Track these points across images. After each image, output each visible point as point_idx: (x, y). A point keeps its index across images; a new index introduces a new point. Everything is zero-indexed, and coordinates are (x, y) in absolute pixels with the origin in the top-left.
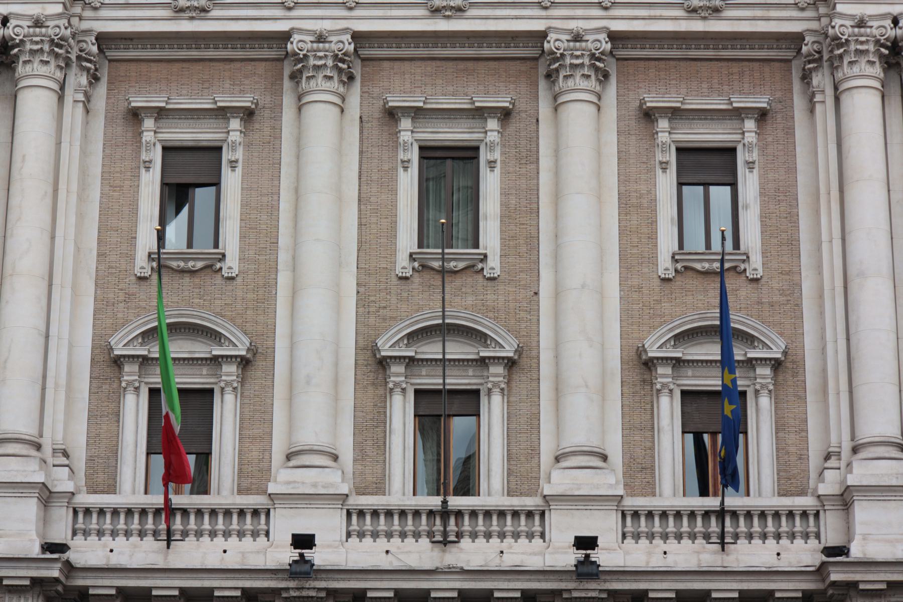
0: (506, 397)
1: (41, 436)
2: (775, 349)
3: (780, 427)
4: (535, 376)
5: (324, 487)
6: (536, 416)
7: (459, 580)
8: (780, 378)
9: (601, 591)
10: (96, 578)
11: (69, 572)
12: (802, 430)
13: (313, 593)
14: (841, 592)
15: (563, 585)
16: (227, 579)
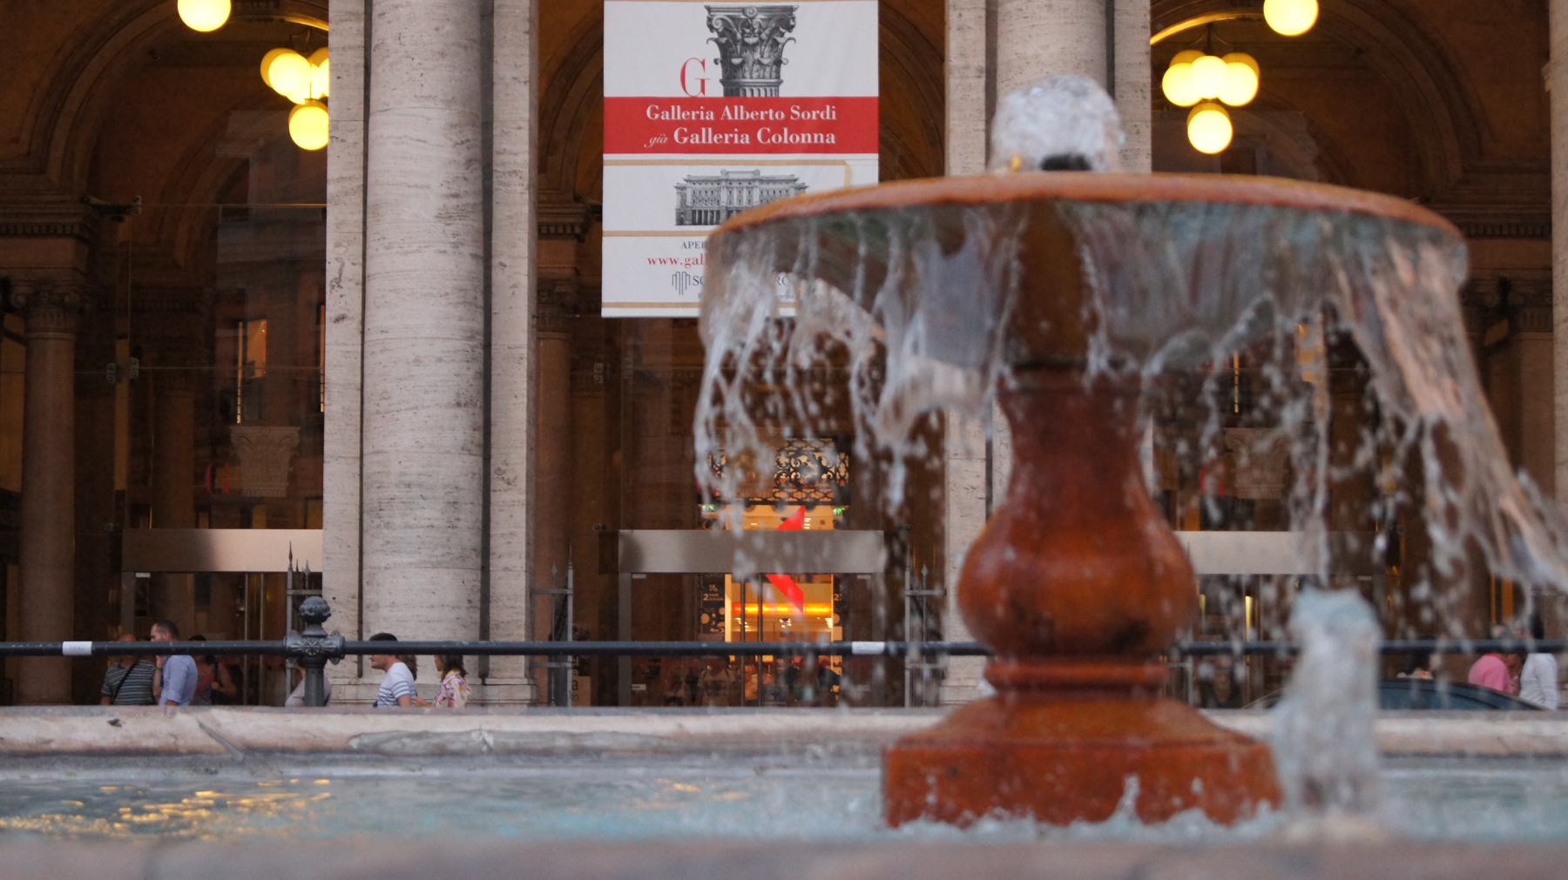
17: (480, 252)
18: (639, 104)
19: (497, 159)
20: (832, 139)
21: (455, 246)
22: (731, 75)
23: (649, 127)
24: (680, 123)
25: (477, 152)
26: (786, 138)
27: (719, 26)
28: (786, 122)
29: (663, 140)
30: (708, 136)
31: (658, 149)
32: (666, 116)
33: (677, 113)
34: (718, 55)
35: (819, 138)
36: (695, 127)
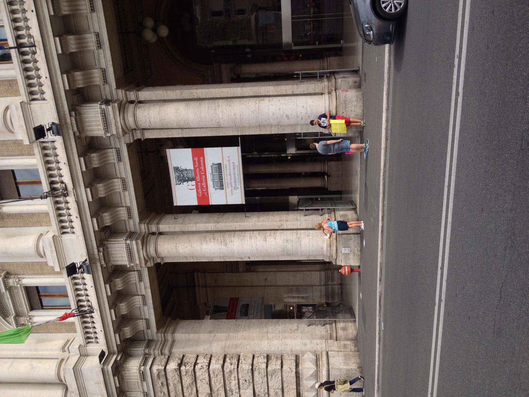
1: (58, 359)
7: (80, 189)
9: (71, 116)
10: (112, 343)
13: (101, 254)
15: (72, 137)
16: (101, 291)
17: (233, 233)
18: (198, 197)
19: (213, 230)
20: (202, 158)
21: (232, 242)
22: (189, 180)
23: (203, 195)
25: (211, 236)
26: (202, 168)
27: (180, 182)
28: (199, 168)
29: (206, 193)
30: (204, 184)
31: (208, 194)
32: (200, 193)
33: (200, 190)
34: (186, 182)
35: (202, 161)
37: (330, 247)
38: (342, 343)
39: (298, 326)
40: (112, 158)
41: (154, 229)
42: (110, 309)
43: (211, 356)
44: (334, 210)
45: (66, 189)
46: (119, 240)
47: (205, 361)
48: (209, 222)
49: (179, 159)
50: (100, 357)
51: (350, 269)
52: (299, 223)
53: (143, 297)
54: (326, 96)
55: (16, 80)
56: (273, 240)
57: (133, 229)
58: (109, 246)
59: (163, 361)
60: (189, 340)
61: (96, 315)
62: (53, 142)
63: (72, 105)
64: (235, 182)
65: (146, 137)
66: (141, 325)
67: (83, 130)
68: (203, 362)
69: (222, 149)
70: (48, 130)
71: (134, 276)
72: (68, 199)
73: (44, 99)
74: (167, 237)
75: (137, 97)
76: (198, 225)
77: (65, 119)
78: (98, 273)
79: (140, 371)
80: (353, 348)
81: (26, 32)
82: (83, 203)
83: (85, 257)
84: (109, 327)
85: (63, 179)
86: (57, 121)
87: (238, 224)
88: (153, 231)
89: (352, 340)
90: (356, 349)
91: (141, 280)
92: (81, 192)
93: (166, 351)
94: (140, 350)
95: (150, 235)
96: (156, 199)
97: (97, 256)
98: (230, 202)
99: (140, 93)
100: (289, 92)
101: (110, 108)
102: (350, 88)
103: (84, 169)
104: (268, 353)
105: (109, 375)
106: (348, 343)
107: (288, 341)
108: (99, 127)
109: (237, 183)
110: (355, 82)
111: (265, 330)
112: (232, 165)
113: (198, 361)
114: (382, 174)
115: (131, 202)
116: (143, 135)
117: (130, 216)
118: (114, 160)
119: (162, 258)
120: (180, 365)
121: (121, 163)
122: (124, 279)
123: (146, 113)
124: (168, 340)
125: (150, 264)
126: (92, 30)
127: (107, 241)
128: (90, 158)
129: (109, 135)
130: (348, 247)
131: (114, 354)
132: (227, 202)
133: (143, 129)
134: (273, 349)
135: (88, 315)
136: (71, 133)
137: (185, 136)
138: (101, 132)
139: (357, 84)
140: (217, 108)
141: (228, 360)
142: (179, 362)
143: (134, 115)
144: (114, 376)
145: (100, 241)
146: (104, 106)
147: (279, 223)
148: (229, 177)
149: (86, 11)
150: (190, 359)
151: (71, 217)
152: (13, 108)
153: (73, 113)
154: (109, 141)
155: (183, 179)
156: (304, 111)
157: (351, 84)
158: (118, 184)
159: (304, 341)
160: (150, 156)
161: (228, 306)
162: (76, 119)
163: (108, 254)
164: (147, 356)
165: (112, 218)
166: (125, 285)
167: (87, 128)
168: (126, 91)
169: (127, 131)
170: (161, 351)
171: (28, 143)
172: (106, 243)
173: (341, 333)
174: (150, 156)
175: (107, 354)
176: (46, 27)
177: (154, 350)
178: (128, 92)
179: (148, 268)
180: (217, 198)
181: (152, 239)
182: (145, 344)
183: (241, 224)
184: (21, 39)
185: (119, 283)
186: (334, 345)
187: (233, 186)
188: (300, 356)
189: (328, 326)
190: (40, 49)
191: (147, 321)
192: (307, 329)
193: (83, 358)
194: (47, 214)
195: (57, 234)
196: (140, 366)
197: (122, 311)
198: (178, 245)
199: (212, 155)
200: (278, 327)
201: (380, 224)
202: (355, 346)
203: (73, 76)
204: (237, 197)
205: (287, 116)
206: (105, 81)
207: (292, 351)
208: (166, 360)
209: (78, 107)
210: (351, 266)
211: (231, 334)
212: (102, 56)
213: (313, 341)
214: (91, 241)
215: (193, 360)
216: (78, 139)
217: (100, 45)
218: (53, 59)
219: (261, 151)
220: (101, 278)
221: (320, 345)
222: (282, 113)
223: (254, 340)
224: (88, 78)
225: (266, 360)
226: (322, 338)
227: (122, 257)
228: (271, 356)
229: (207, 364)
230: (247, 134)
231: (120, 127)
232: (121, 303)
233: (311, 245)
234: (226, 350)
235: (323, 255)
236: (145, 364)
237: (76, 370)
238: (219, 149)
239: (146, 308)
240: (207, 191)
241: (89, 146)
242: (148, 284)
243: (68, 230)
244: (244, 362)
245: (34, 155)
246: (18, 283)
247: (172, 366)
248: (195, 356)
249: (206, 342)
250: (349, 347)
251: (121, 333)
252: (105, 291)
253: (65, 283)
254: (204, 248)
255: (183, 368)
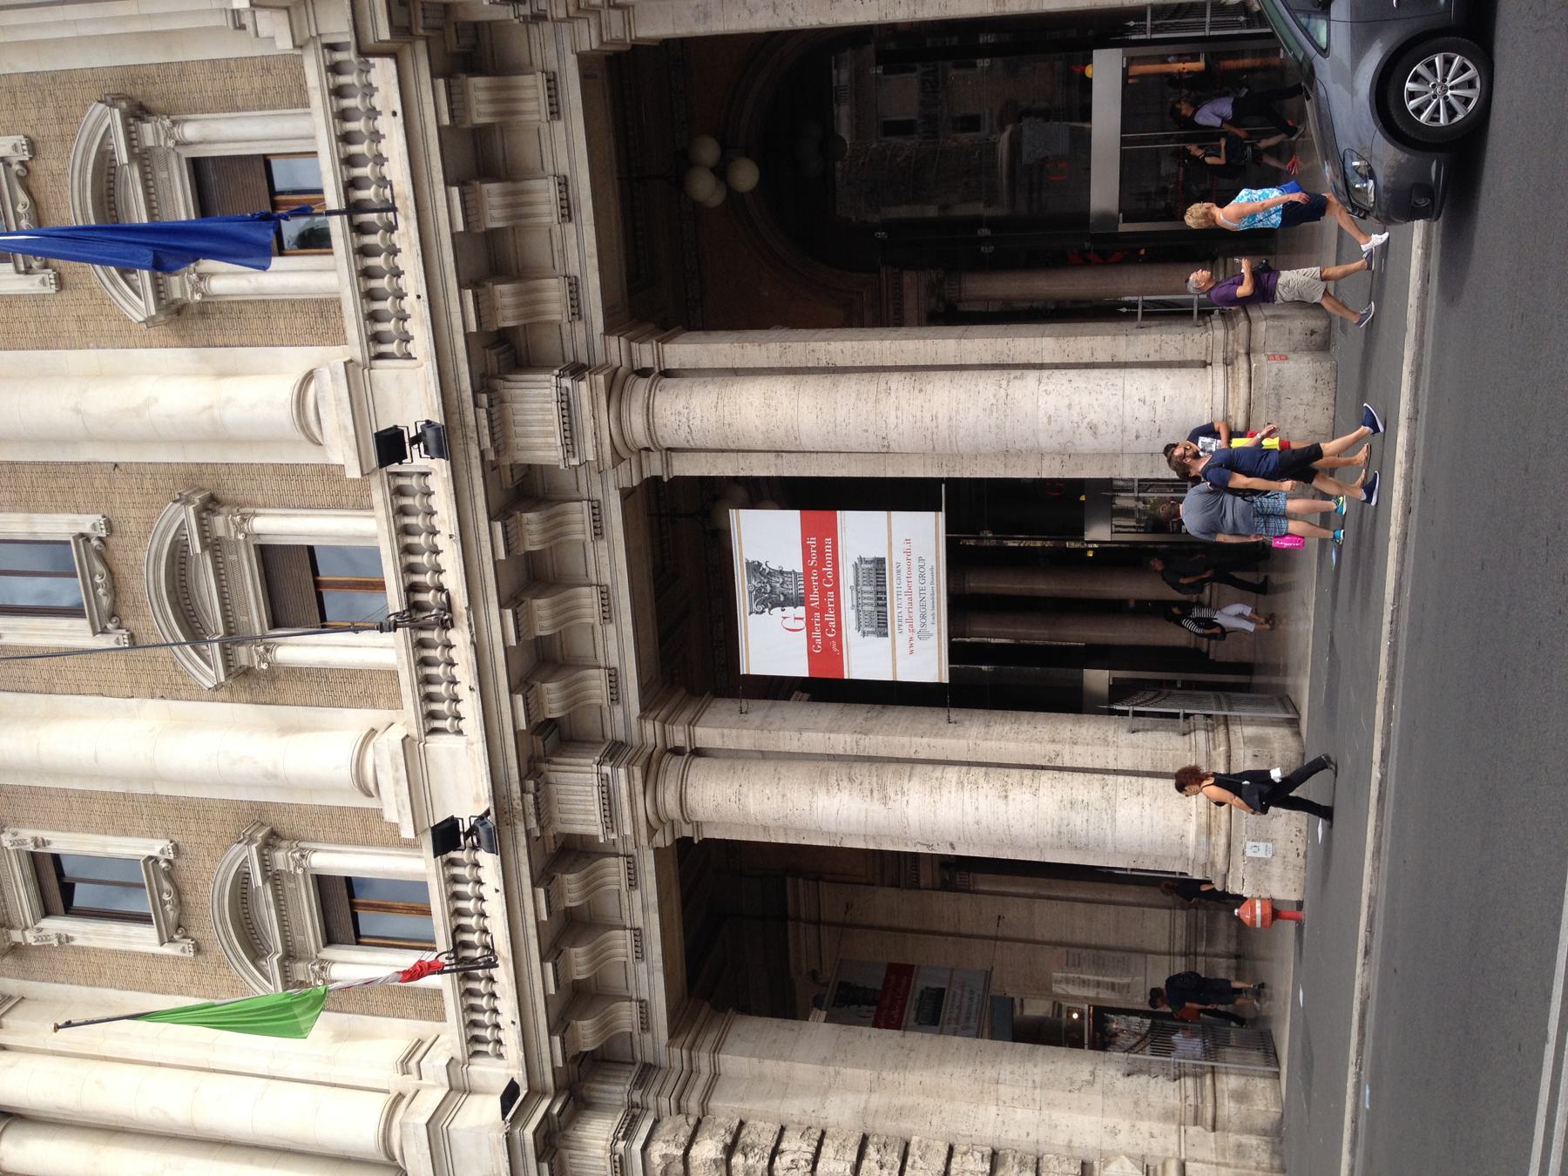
0: (259, 511)
1: (387, 1092)
2: (108, 120)
3: (229, 104)
4: (225, 469)
5: (397, 770)
6: (277, 468)
7: (487, 609)
8: (159, 104)
9: (476, 405)
10: (541, 1062)
11: (537, 1092)
12: (228, 66)
13: (531, 797)
14: (420, 14)
15: (476, 463)
16: (522, 906)
17: (908, 767)
23: (826, 648)
24: (823, 633)
26: (829, 569)
27: (761, 608)
30: (830, 617)
31: (840, 647)
33: (817, 634)
36: (825, 625)
37: (1209, 833)
38: (1233, 1138)
39: (1093, 1073)
40: (579, 527)
41: (679, 737)
42: (543, 960)
43: (823, 1133)
44: (1226, 721)
45: (449, 607)
46: (582, 761)
47: (804, 1147)
48: (838, 731)
49: (765, 538)
50: (502, 1098)
51: (1269, 911)
52: (1112, 752)
53: (638, 933)
54: (1218, 372)
55: (338, 300)
56: (1028, 796)
57: (621, 736)
58: (552, 777)
59: (681, 1133)
60: (761, 1078)
61: (503, 975)
62: (425, 474)
63: (483, 376)
64: (923, 617)
65: (676, 473)
66: (627, 1016)
67: (506, 445)
68: (797, 1147)
69: (889, 518)
70: (415, 440)
71: (615, 870)
72: (453, 635)
73: (408, 356)
74: (716, 763)
75: (659, 358)
76: (805, 735)
77: (462, 414)
78: (516, 851)
79: (613, 1153)
80: (1265, 1158)
81: (373, 170)
82: (492, 652)
83: (486, 804)
84: (535, 1012)
85: (442, 578)
86: (438, 419)
87: (925, 740)
88: (678, 744)
89: (1264, 1133)
90: (1276, 1163)
91: (633, 883)
92: (488, 615)
93: (693, 1104)
94: (617, 1091)
95: (668, 756)
96: (692, 650)
97: (517, 803)
98: (904, 676)
99: (667, 347)
100: (1102, 357)
101: (584, 386)
102: (1295, 351)
103: (502, 555)
104: (997, 1146)
105: (524, 1155)
106: (1253, 1140)
107: (1060, 1117)
108: (552, 440)
109: (929, 618)
110: (1313, 333)
111: (990, 1073)
112: (915, 564)
113: (784, 1146)
114: (1387, 618)
115: (621, 657)
116: (667, 464)
117: (616, 697)
118: (584, 532)
119: (698, 825)
120: (730, 1150)
121: (603, 544)
122: (586, 877)
123: (680, 404)
124: (699, 1072)
125: (664, 840)
126: (549, 169)
127: (548, 762)
128: (519, 523)
129: (575, 462)
130: (1267, 840)
131: (544, 1094)
132: (895, 673)
133: (669, 449)
134: (1011, 1135)
135: (480, 972)
136: (474, 452)
137: (786, 474)
138: (554, 453)
139: (1317, 338)
140: (883, 396)
141: (871, 1150)
142: (729, 1140)
143: (649, 410)
144: (539, 1159)
145: (529, 761)
146: (567, 382)
147: (1051, 747)
148: (905, 599)
149: (537, 117)
150: (761, 1135)
151: (457, 688)
152: (325, 375)
153: (484, 398)
154: (573, 481)
155: (769, 600)
156: (1144, 414)
157: (1298, 336)
158: (588, 600)
159: (1110, 1121)
160: (683, 524)
161: (879, 987)
162: (489, 414)
163: (548, 800)
164: (637, 1111)
165: (568, 697)
166: (587, 894)
167: (517, 440)
168: (631, 340)
169: (624, 454)
170: (678, 1101)
171: (357, 475)
172: (544, 767)
173: (1229, 1108)
174: (683, 524)
175: (523, 1092)
176: (428, 156)
177: (658, 1095)
178: (634, 345)
179: (657, 850)
180: (866, 660)
181: (674, 765)
182: (631, 1074)
183: (933, 741)
184: (359, 188)
185: (572, 888)
186: (1203, 1143)
187: (917, 627)
188: (1096, 1165)
189: (1189, 1082)
190: (406, 218)
191: (644, 1007)
192: (1122, 1084)
193: (457, 1098)
194: (393, 674)
195: (414, 732)
196: (616, 1139)
197: (548, 706)
198: (744, 790)
199: (861, 533)
200: (1029, 1066)
201: (1376, 774)
202: (1274, 1153)
203: (491, 297)
204: (925, 661)
205: (1093, 428)
206: (577, 311)
207: (1069, 1146)
208: (690, 1131)
209: (499, 383)
210: (1272, 900)
211: (884, 1074)
212: (572, 242)
213: (1138, 1124)
214: (505, 760)
215: (768, 1141)
216: (490, 469)
217: (567, 212)
218: (439, 245)
219: (1007, 531)
220: (525, 869)
221: (1163, 1141)
222: (1076, 419)
223: (952, 1099)
224: (530, 304)
225: (987, 1167)
226: (1167, 1116)
227: (587, 812)
228: (1005, 1156)
229: (809, 1157)
230: (966, 475)
231: (607, 441)
232: (573, 945)
233: (1147, 822)
234: (869, 1121)
235: (1183, 857)
236: (628, 1133)
237: (436, 1128)
238: (879, 517)
239: (642, 967)
240: (839, 638)
241: (520, 491)
242: (653, 898)
243: (446, 724)
244: (920, 1163)
245: (372, 508)
246: (239, 530)
247: (708, 1149)
248: (777, 1128)
249: (810, 1090)
250: (1255, 1154)
251: (568, 1035)
252: (533, 905)
253: (425, 875)
254: (820, 804)
255: (738, 1160)
